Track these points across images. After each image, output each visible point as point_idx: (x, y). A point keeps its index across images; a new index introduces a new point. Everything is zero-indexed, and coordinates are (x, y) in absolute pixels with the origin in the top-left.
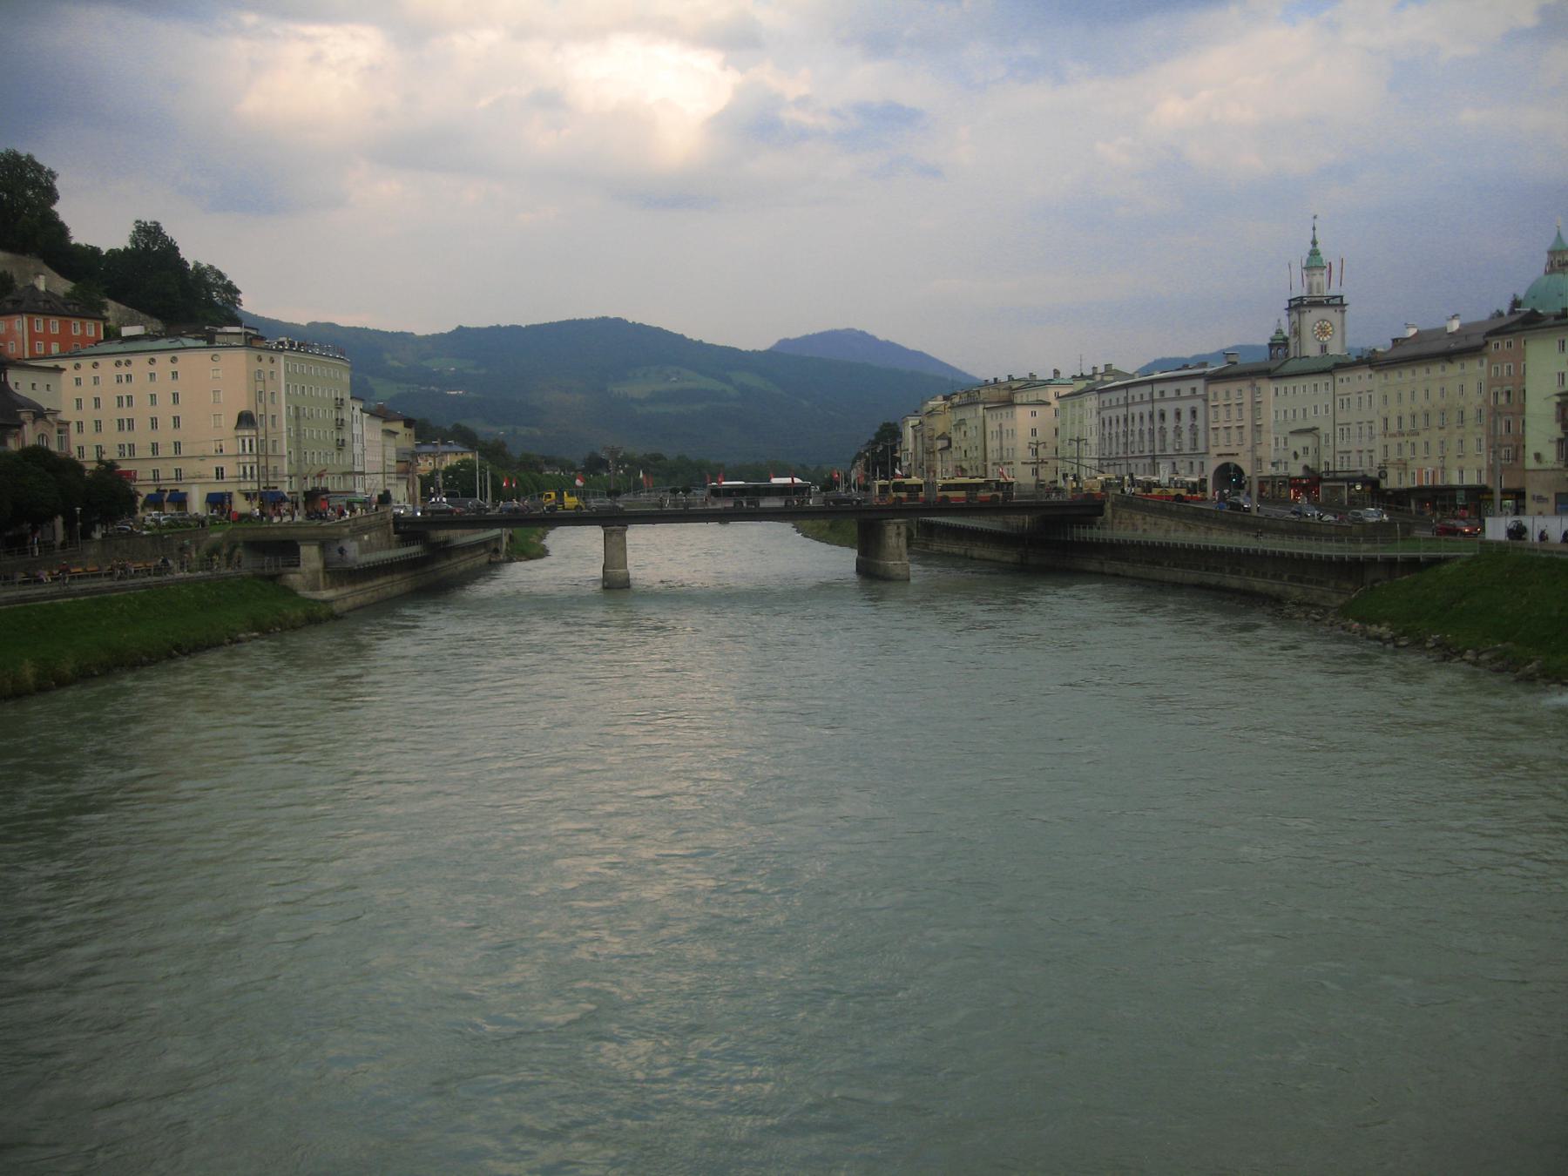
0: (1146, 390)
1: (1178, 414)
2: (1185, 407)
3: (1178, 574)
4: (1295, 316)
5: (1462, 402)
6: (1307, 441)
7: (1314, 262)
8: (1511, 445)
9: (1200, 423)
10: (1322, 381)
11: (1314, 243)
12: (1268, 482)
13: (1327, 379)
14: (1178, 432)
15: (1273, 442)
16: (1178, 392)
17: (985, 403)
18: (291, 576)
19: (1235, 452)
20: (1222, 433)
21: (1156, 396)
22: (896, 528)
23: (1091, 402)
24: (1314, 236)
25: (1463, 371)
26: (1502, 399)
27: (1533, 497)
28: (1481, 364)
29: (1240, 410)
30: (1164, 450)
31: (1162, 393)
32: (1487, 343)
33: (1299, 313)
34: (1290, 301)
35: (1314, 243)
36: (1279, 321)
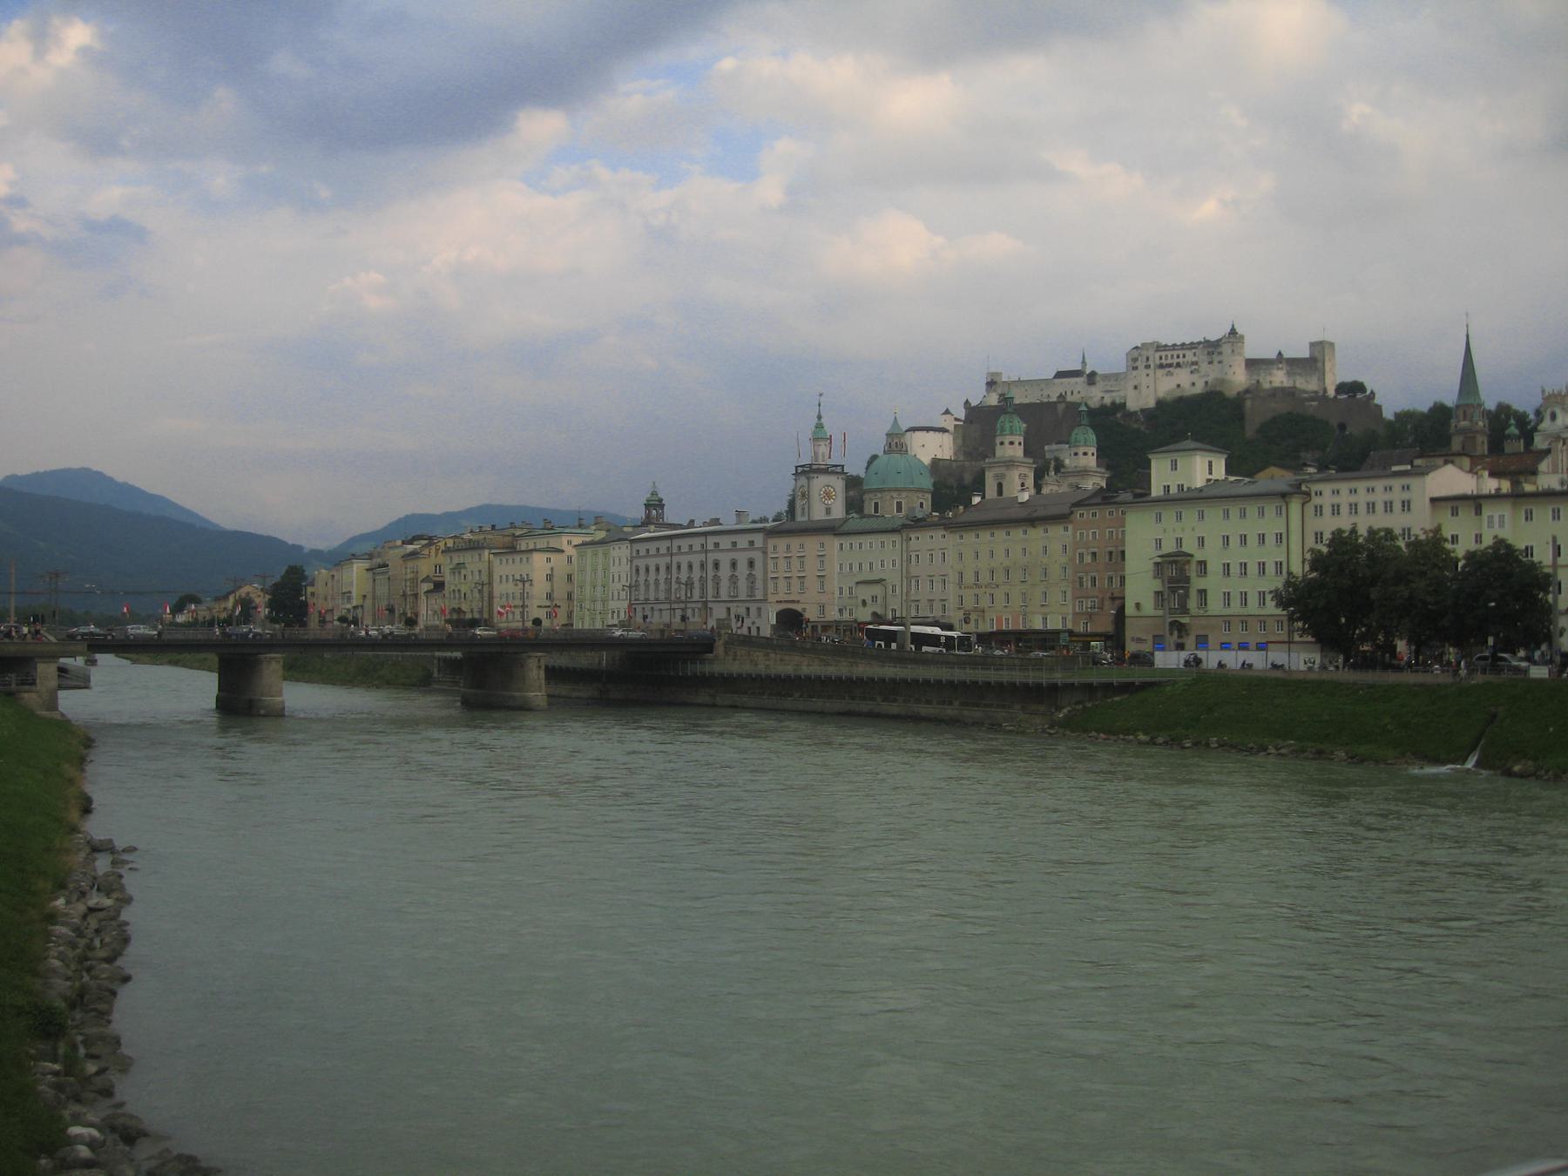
0: (697, 543)
1: (734, 565)
2: (725, 559)
3: (818, 704)
4: (803, 481)
5: (1045, 561)
6: (877, 590)
7: (819, 435)
8: (1097, 597)
9: (758, 571)
10: (888, 539)
11: (819, 417)
12: (830, 627)
13: (896, 537)
14: (733, 580)
16: (734, 544)
17: (490, 549)
18: (26, 695)
19: (796, 599)
20: (782, 584)
21: (710, 547)
22: (537, 660)
23: (621, 552)
25: (1025, 536)
26: (1088, 559)
27: (1133, 639)
28: (1066, 529)
29: (802, 564)
30: (691, 597)
31: (717, 545)
32: (1072, 512)
33: (808, 479)
34: (797, 467)
35: (819, 417)
36: (654, 483)
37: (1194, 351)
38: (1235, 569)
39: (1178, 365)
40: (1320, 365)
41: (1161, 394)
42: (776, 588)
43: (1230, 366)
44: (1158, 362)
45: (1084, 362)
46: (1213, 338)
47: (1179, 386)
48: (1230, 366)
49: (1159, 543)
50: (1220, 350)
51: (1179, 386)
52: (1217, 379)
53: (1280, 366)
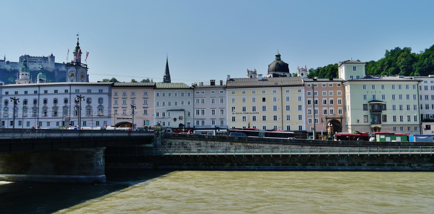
6: (182, 114)
11: (78, 44)
15: (155, 115)
24: (78, 41)
35: (78, 44)
37: (40, 59)
38: (398, 107)
39: (35, 62)
42: (116, 111)
43: (51, 64)
44: (29, 61)
45: (5, 58)
46: (45, 56)
47: (35, 68)
48: (51, 64)
49: (365, 97)
50: (48, 60)
51: (35, 68)
52: (47, 67)
53: (64, 65)
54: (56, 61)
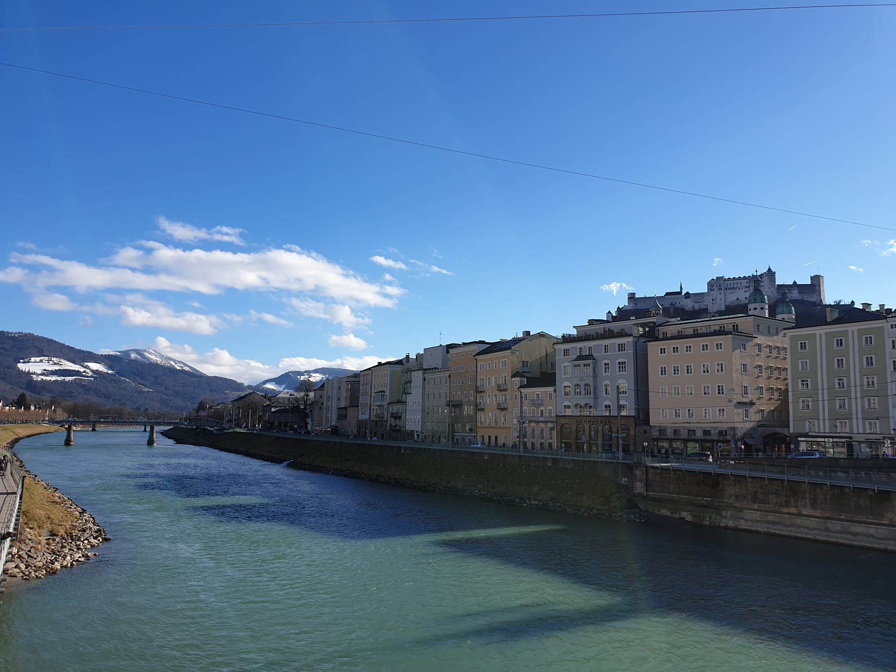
40: (817, 288)
41: (728, 304)
43: (769, 288)
45: (681, 288)
47: (738, 299)
48: (769, 288)
51: (738, 299)
53: (796, 288)
54: (779, 282)
